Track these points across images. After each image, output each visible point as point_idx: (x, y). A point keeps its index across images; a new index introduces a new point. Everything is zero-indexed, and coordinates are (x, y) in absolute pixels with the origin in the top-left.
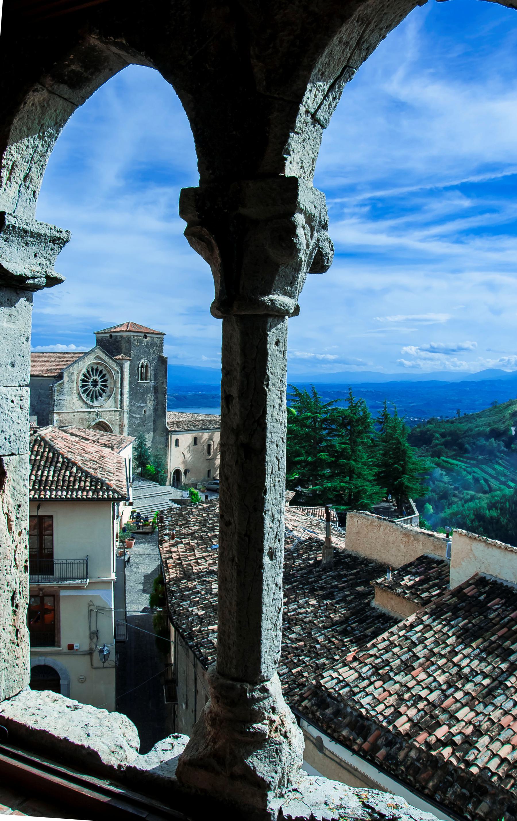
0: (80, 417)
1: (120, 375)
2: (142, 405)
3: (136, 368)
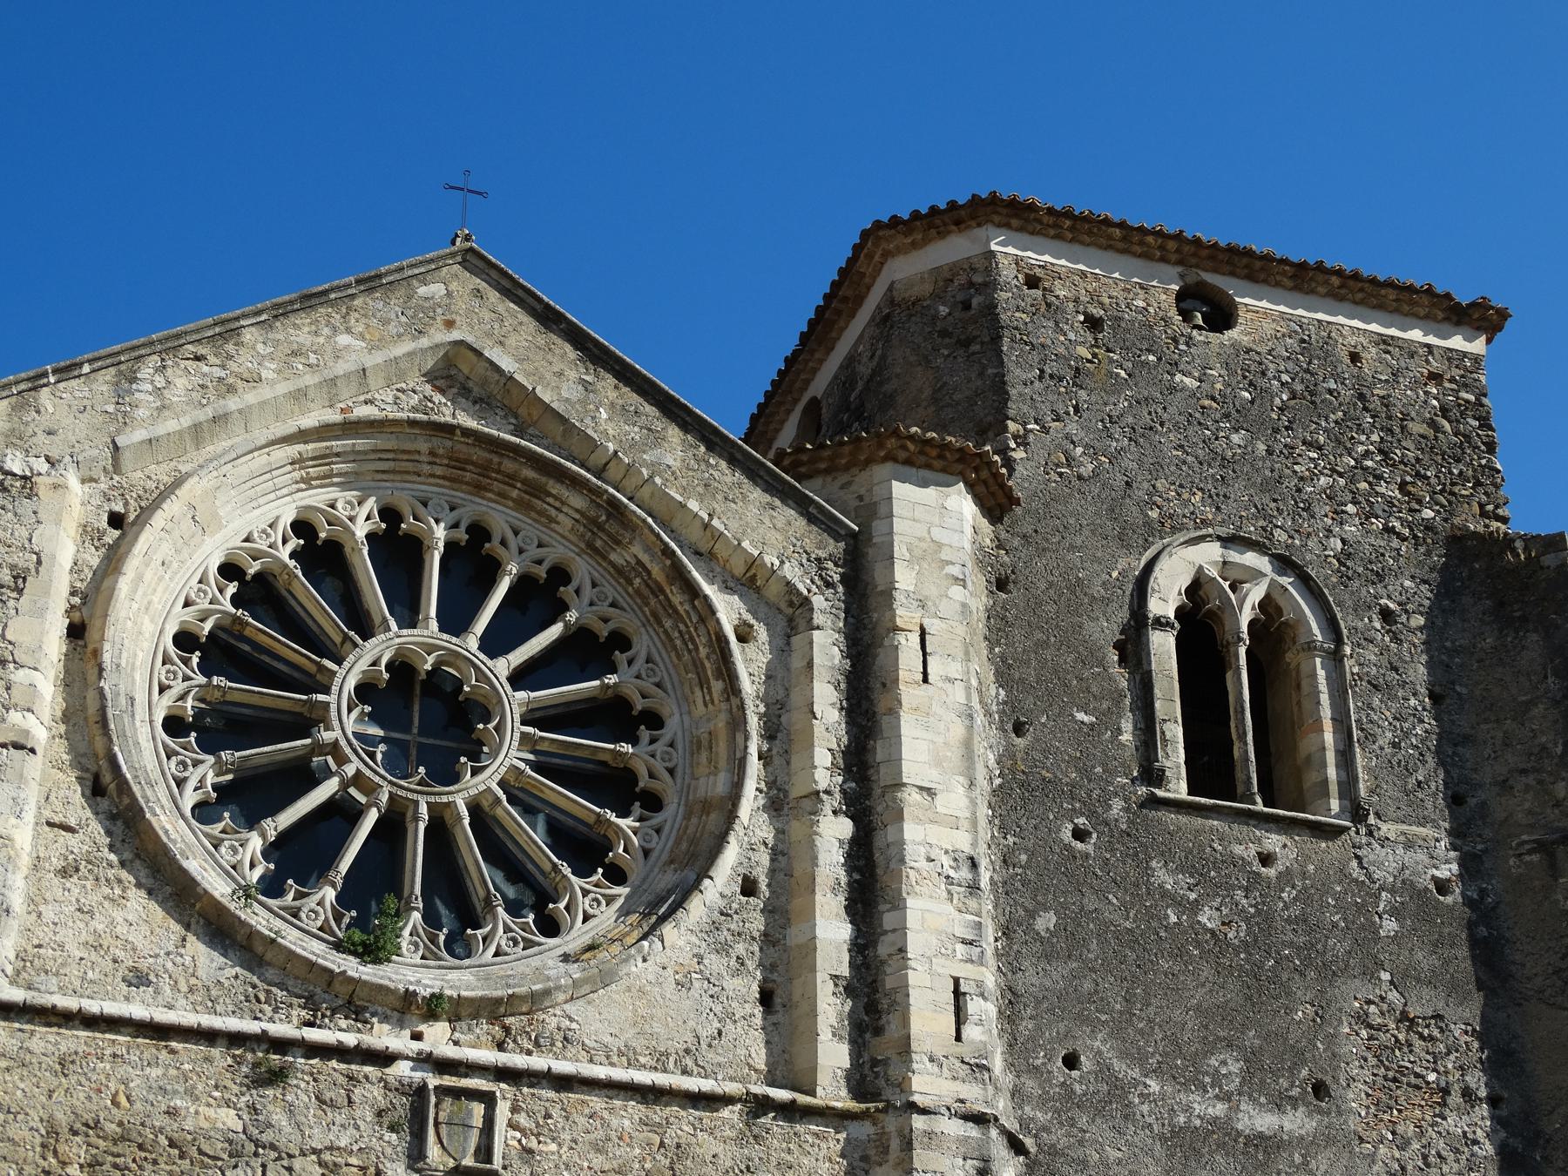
0: (76, 1099)
1: (826, 648)
2: (1258, 1120)
3: (1106, 628)
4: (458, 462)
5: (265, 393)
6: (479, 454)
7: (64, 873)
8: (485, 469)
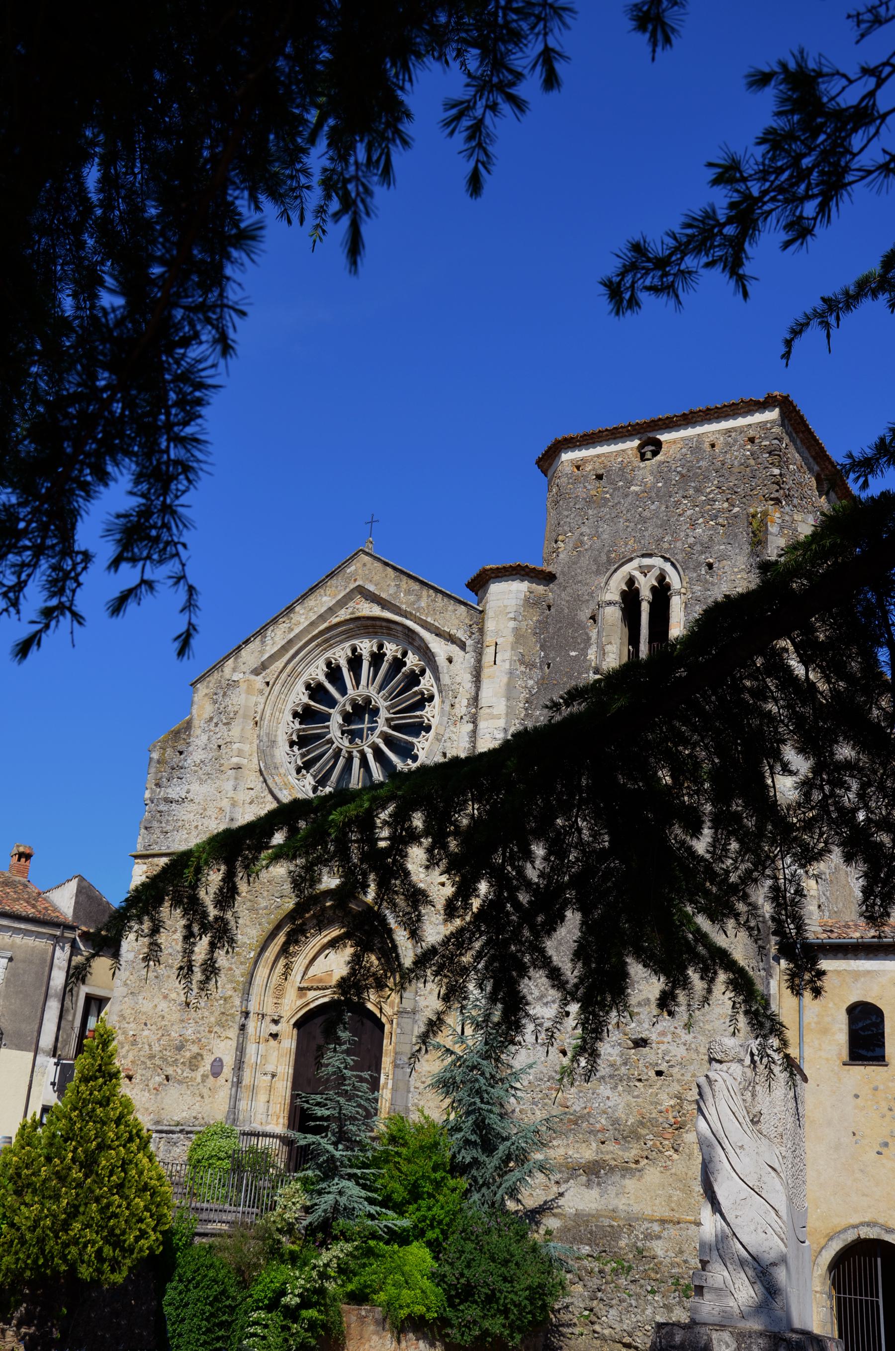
4: (366, 627)
5: (301, 627)
6: (369, 623)
7: (251, 803)
8: (374, 626)
